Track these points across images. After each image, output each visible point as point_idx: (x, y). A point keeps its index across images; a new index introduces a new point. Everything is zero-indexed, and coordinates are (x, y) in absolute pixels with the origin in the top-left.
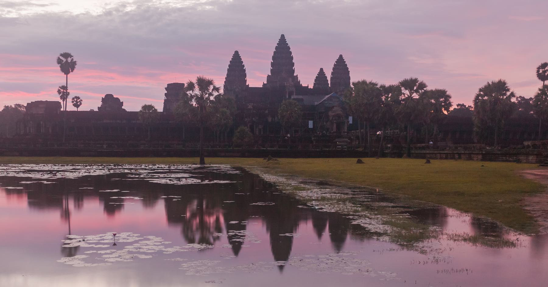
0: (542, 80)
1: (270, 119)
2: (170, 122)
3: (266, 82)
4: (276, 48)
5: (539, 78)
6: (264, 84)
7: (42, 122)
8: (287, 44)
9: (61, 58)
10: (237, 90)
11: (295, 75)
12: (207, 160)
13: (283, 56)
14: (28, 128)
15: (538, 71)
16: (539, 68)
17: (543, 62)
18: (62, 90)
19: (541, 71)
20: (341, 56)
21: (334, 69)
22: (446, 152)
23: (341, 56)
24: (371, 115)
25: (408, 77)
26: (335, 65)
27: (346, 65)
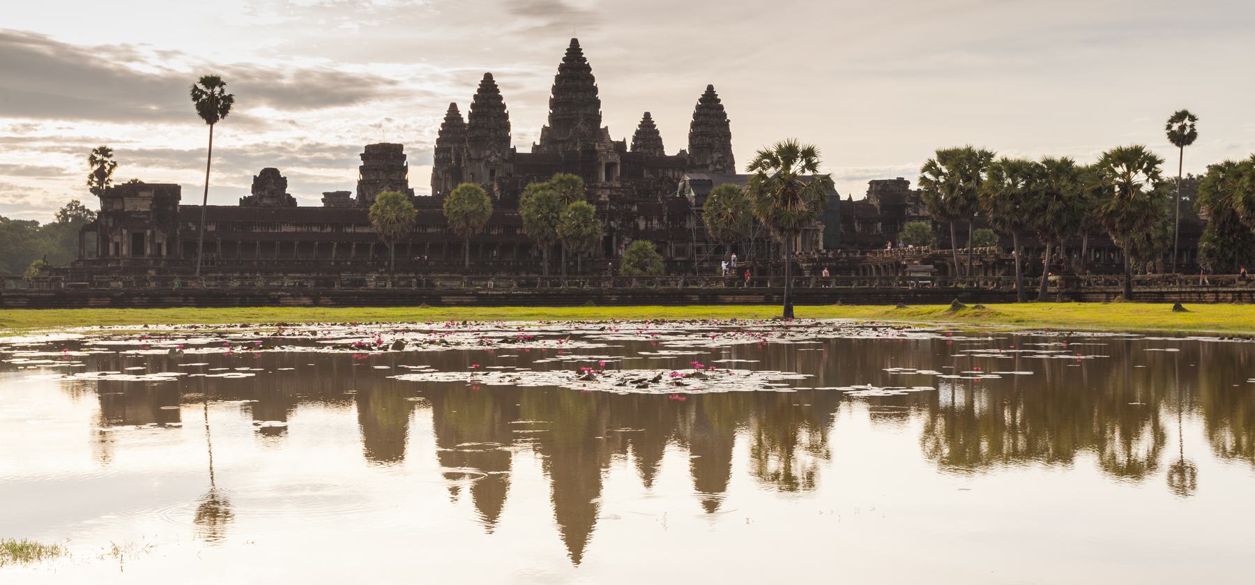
0: (1178, 145)
1: (642, 225)
2: (429, 230)
3: (538, 143)
4: (562, 68)
5: (1173, 141)
6: (535, 147)
7: (149, 232)
8: (585, 59)
9: (201, 87)
10: (493, 159)
11: (602, 126)
12: (797, 310)
13: (575, 84)
14: (111, 245)
15: (1169, 127)
16: (1172, 120)
17: (1180, 110)
18: (99, 157)
19: (1175, 127)
20: (710, 88)
21: (696, 116)
22: (1238, 289)
23: (710, 88)
24: (1026, 217)
25: (1126, 145)
26: (698, 107)
27: (722, 107)
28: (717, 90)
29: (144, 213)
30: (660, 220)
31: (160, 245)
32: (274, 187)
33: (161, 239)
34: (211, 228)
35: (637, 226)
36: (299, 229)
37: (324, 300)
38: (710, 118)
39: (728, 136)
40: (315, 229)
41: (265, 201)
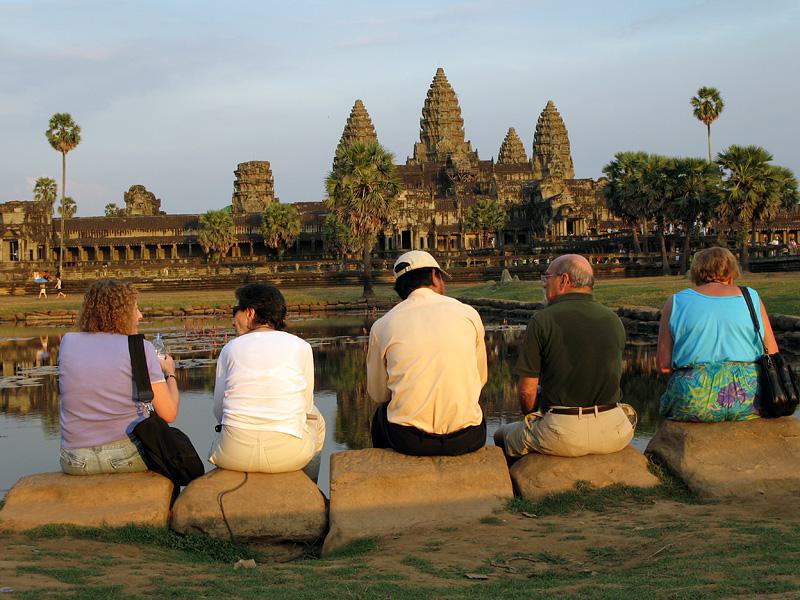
1: (439, 220)
4: (430, 93)
6: (409, 160)
11: (466, 140)
28: (560, 107)
29: (17, 226)
30: (455, 215)
31: (31, 251)
32: (140, 201)
33: (33, 246)
34: (74, 236)
35: (433, 221)
36: (145, 234)
37: (20, 291)
38: (549, 125)
39: (567, 143)
40: (160, 234)
41: (134, 213)
